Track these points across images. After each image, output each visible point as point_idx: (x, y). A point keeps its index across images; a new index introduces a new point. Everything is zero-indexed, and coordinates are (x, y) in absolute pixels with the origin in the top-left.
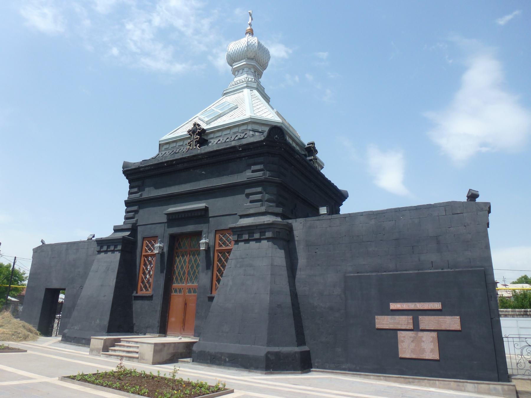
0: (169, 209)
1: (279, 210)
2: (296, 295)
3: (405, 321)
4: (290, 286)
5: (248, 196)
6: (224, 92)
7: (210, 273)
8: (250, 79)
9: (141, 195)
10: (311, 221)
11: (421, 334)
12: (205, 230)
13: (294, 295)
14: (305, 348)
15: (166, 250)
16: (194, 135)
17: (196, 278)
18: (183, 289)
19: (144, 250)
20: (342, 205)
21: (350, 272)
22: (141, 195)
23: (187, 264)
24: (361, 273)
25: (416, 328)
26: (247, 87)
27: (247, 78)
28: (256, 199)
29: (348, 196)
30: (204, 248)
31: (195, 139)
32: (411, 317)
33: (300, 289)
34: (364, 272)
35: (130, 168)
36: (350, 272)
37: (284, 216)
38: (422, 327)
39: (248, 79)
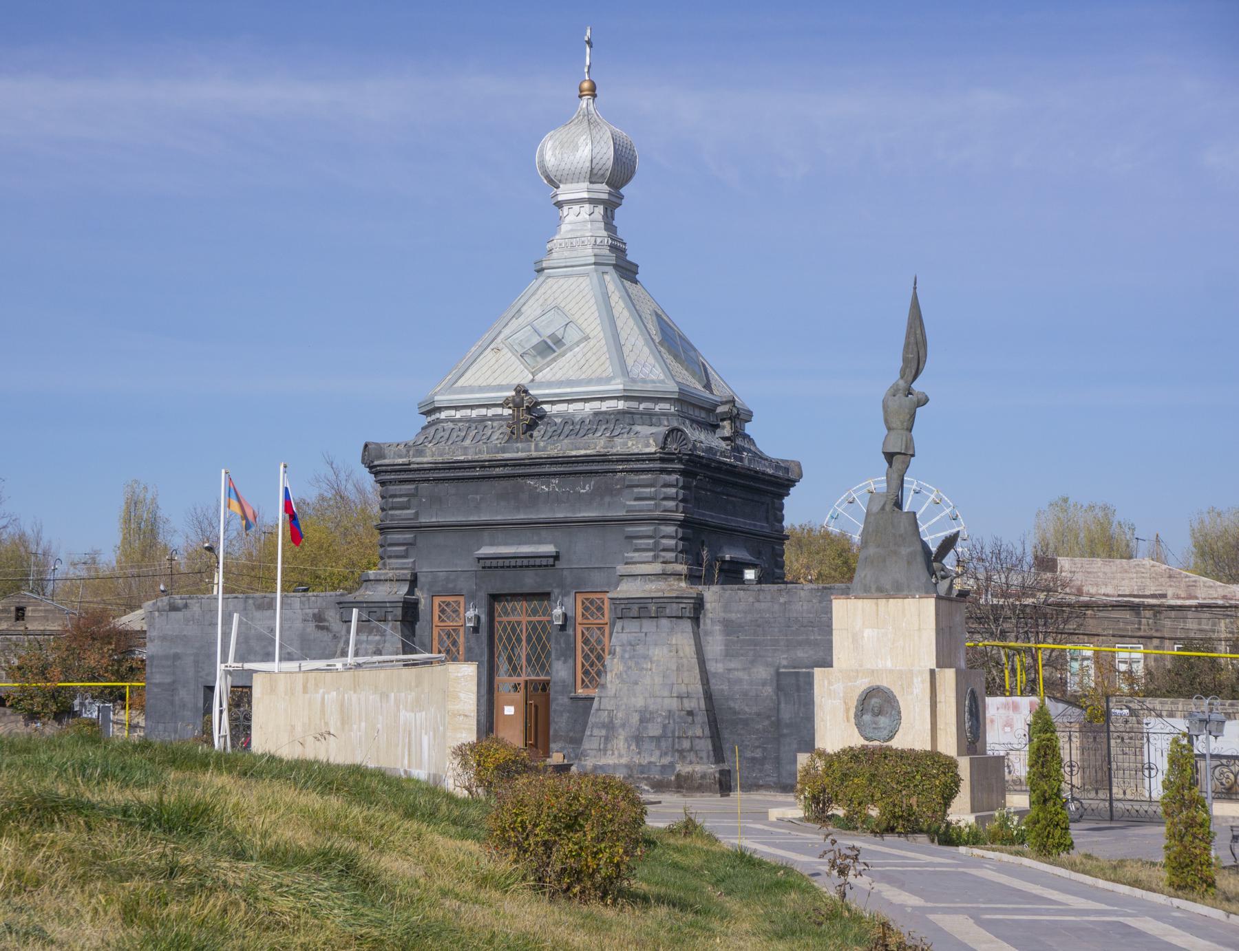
0: (479, 549)
1: (682, 568)
2: (711, 695)
4: (703, 685)
5: (630, 538)
6: (544, 265)
7: (571, 661)
8: (599, 240)
9: (417, 515)
10: (731, 590)
12: (556, 591)
13: (708, 696)
14: (726, 767)
15: (484, 618)
16: (518, 411)
17: (543, 667)
18: (519, 684)
19: (436, 618)
20: (788, 494)
21: (785, 667)
22: (417, 515)
23: (524, 643)
24: (799, 668)
26: (595, 264)
27: (594, 238)
28: (643, 547)
29: (801, 476)
30: (560, 623)
31: (523, 420)
33: (717, 686)
34: (802, 668)
35: (387, 461)
36: (785, 667)
37: (693, 578)
39: (595, 241)
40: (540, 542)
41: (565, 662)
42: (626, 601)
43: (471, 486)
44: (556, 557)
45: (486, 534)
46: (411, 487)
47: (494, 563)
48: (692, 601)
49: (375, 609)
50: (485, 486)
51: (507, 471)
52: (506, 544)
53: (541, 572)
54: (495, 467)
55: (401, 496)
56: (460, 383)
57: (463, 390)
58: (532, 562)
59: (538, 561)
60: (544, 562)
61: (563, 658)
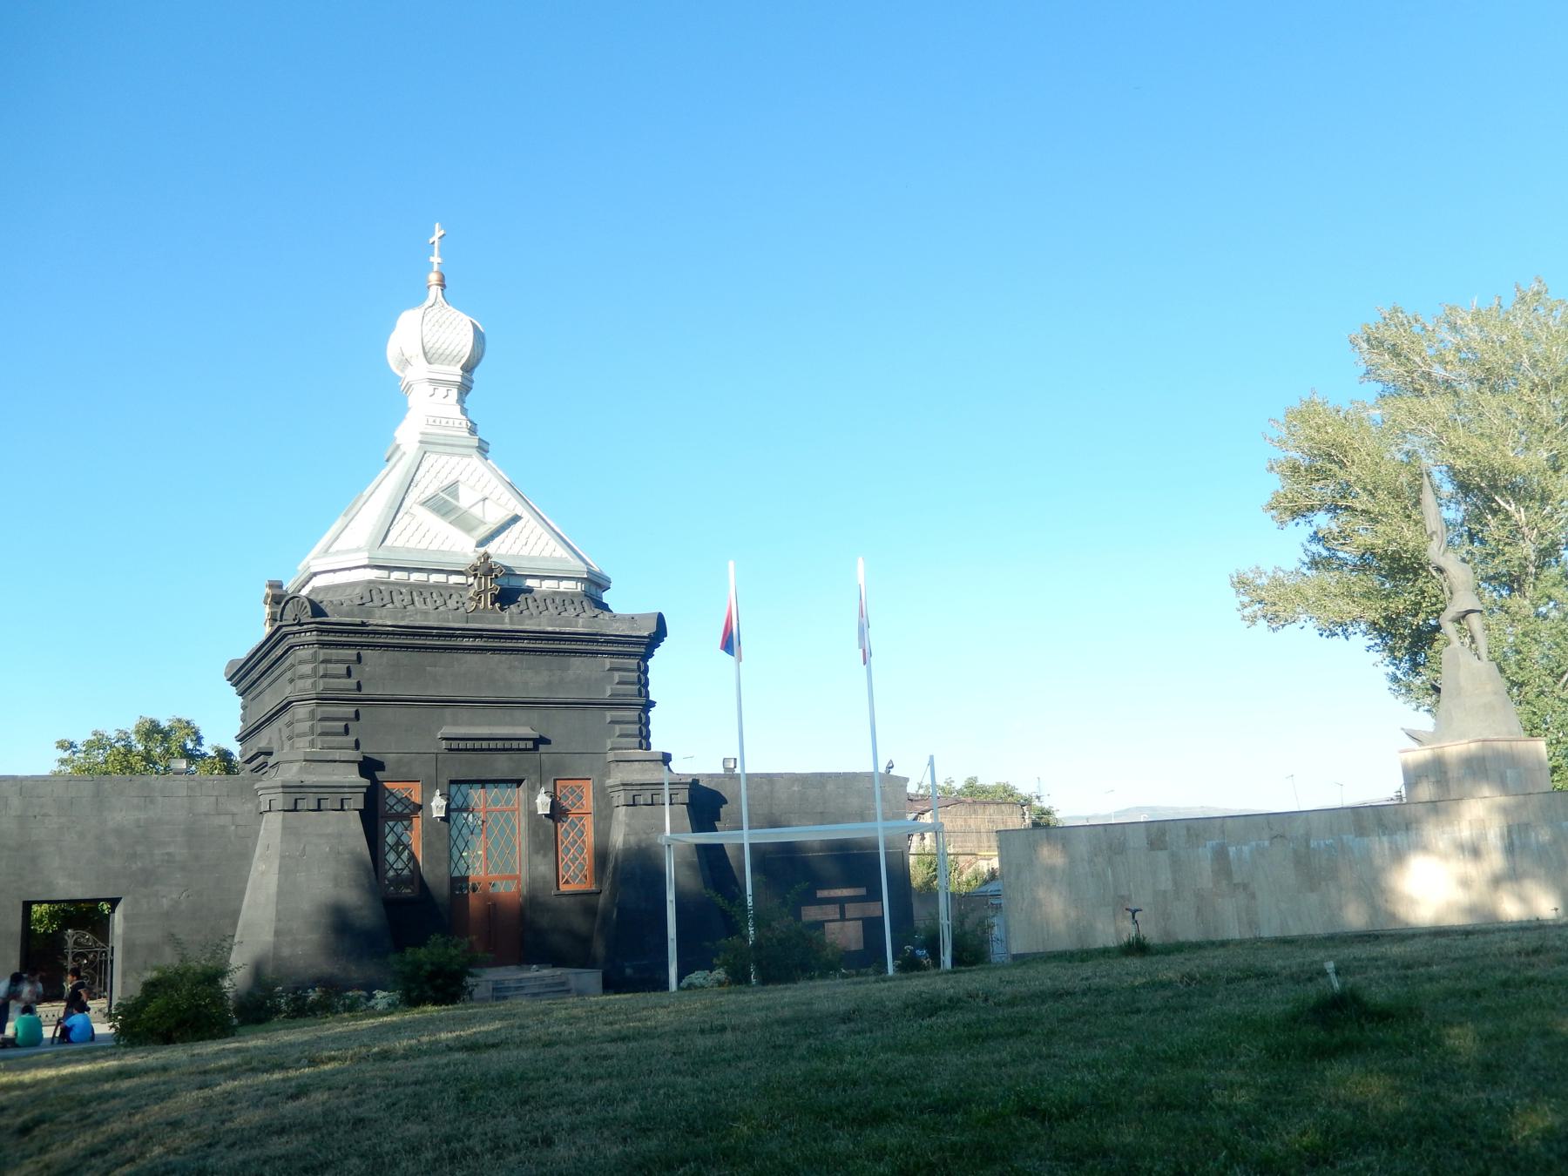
3: (832, 911)
11: (847, 923)
18: (479, 884)
22: (359, 687)
25: (843, 918)
32: (838, 905)
38: (847, 916)
40: (513, 724)
41: (545, 856)
42: (639, 788)
43: (428, 657)
44: (540, 741)
45: (448, 712)
46: (351, 653)
47: (462, 745)
48: (688, 786)
49: (325, 796)
50: (445, 657)
51: (478, 642)
52: (471, 724)
53: (516, 756)
54: (464, 637)
55: (337, 662)
56: (388, 542)
57: (391, 549)
58: (507, 745)
59: (515, 745)
60: (522, 745)
61: (542, 852)
